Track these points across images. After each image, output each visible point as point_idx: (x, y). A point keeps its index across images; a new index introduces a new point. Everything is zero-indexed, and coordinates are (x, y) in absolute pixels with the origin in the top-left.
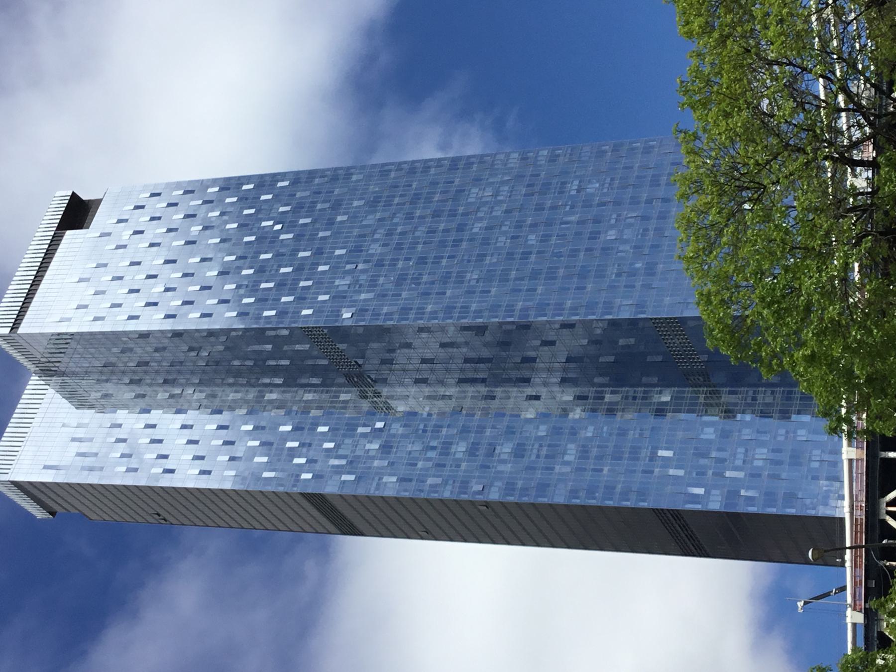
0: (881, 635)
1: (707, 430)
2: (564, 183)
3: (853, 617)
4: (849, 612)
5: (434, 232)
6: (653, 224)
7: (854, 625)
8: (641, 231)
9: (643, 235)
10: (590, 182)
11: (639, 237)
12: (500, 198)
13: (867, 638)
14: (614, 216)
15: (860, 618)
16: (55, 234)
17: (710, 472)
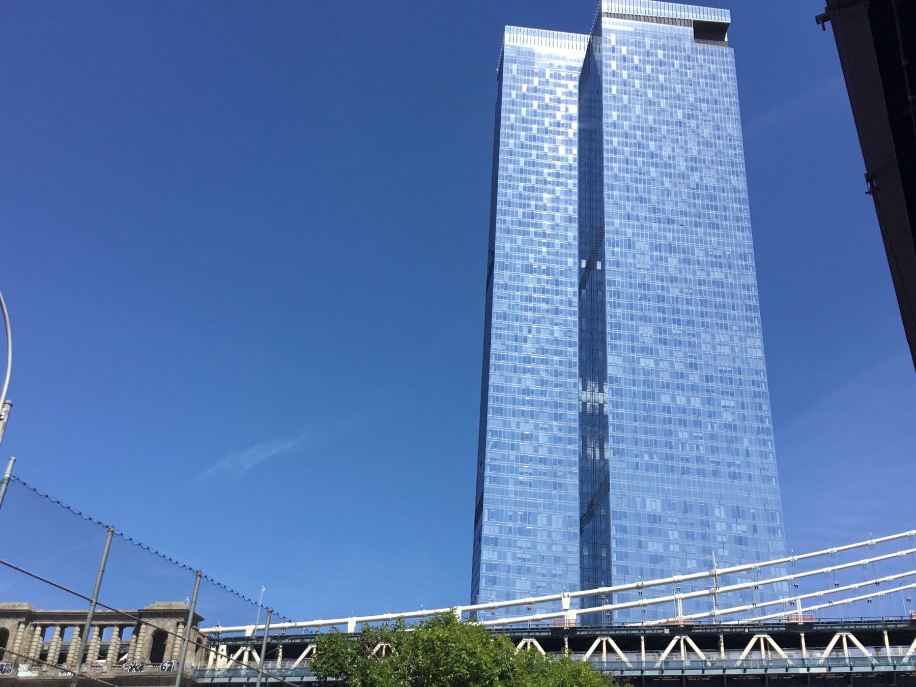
0: (238, 648)
1: (545, 520)
2: (732, 394)
3: (249, 631)
4: (253, 627)
5: (687, 303)
6: (694, 466)
7: (244, 631)
8: (687, 457)
9: (682, 459)
10: (733, 414)
11: (681, 456)
12: (718, 347)
13: (236, 639)
14: (700, 435)
15: (248, 634)
16: (691, 20)
17: (511, 524)
